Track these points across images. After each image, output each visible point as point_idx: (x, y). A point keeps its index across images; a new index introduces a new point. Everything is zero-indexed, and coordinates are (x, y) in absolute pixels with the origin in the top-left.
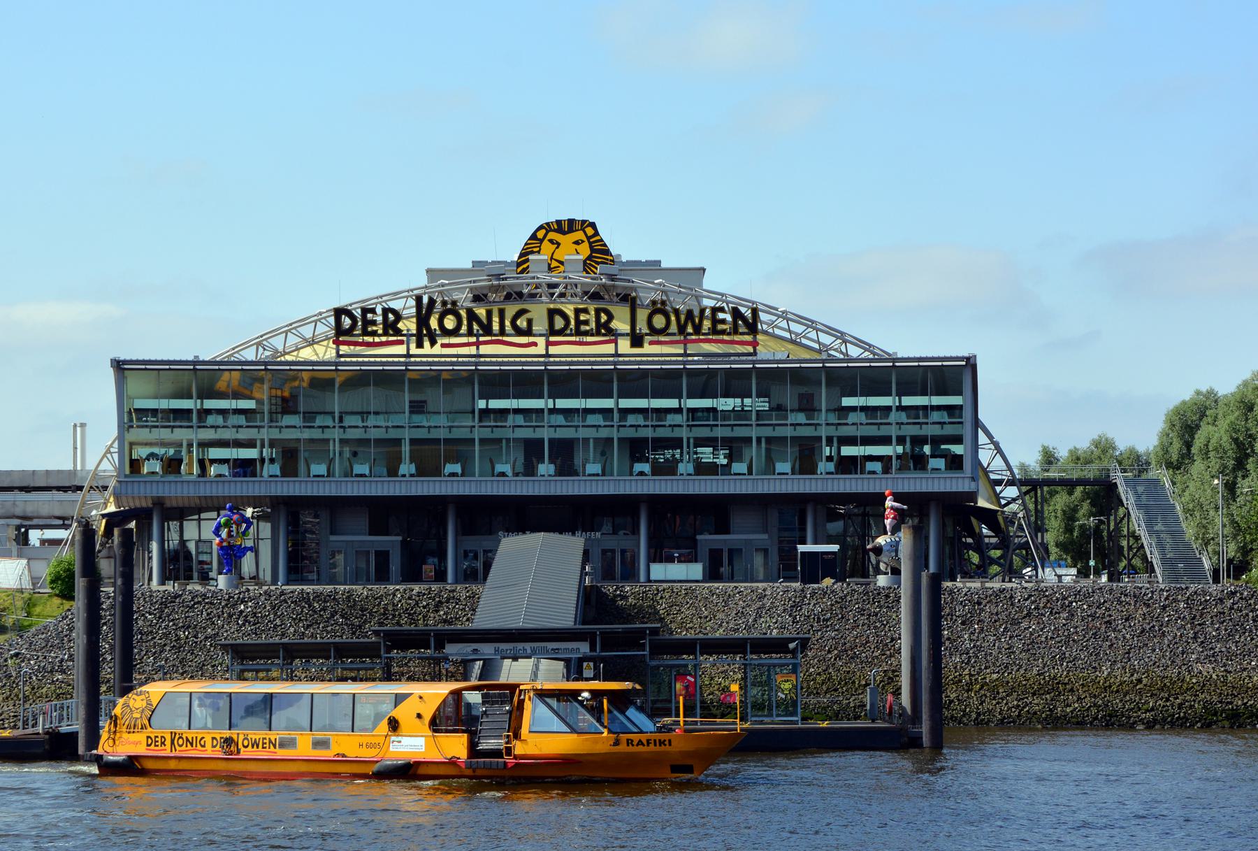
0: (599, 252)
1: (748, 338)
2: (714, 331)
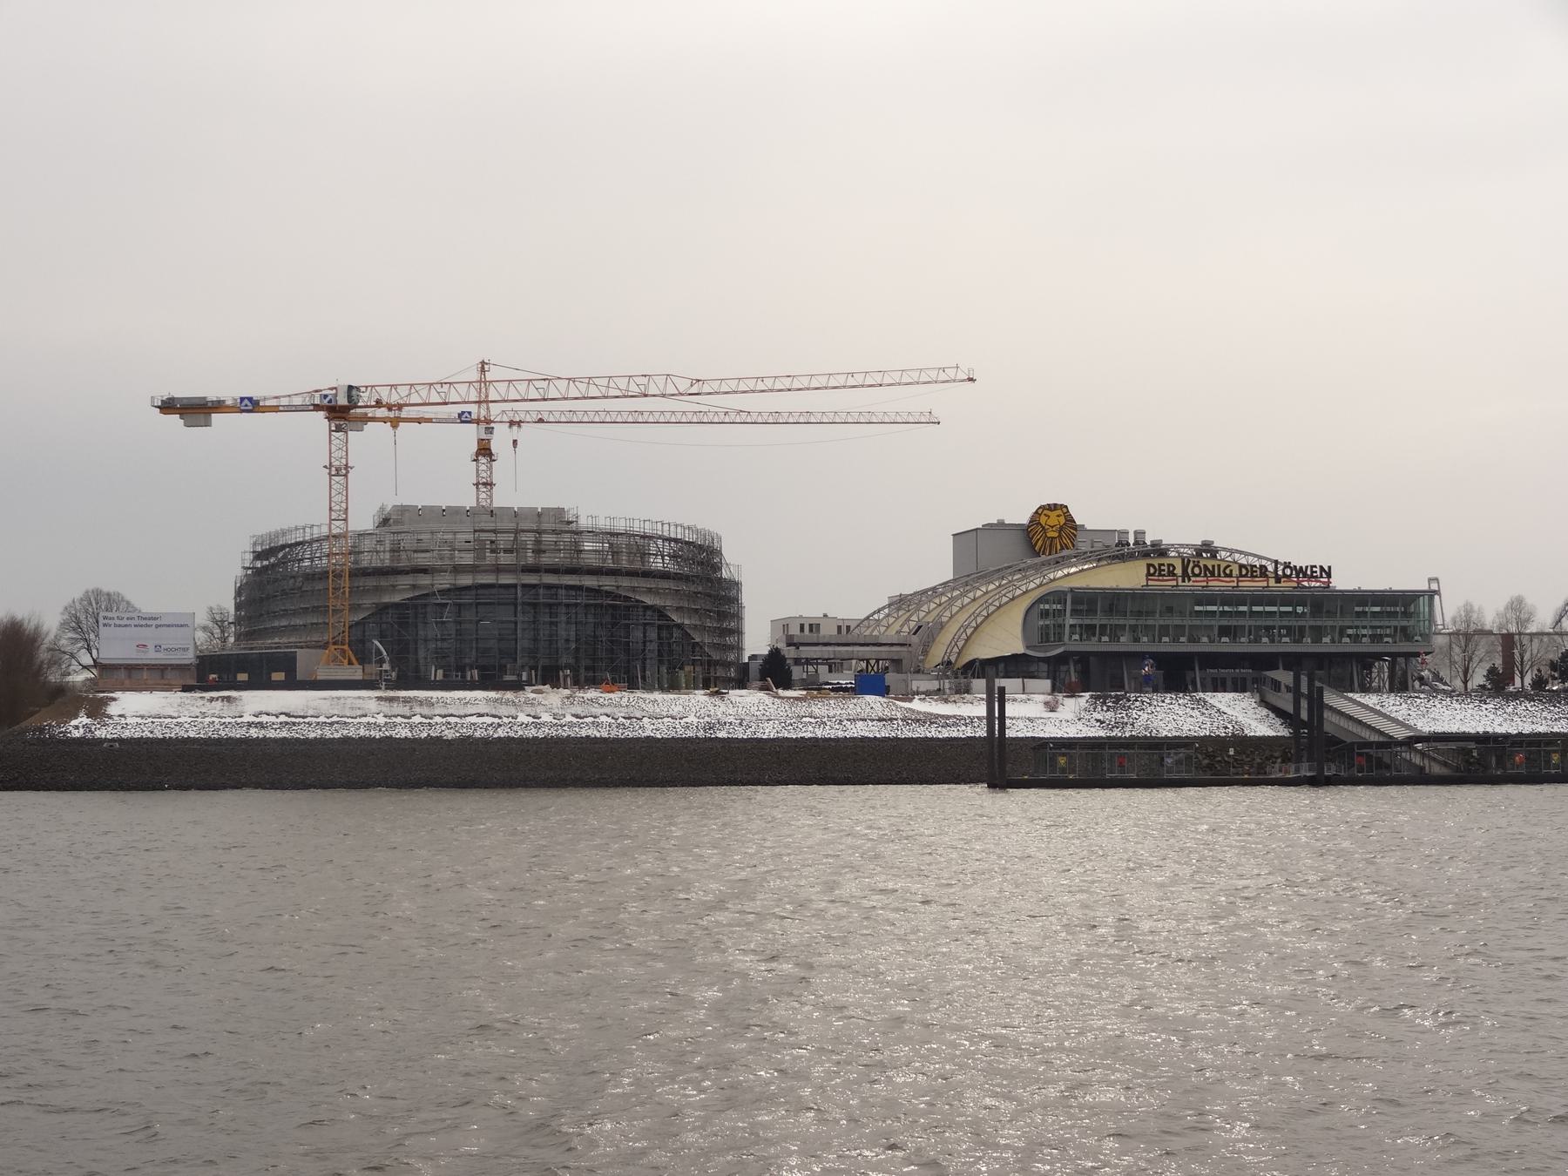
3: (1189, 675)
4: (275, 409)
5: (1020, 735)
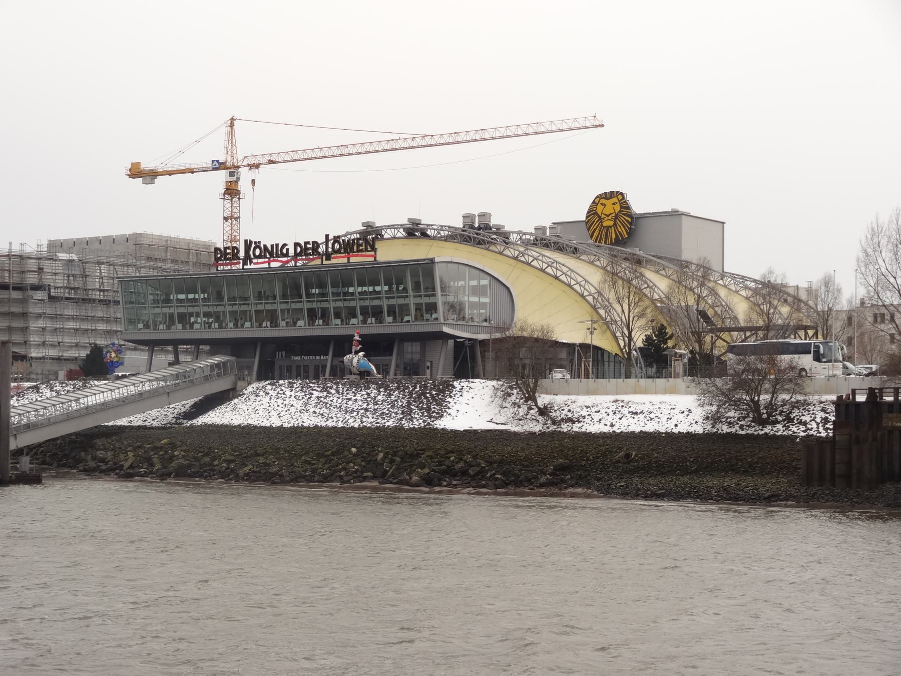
0: (625, 206)
1: (373, 253)
2: (358, 251)
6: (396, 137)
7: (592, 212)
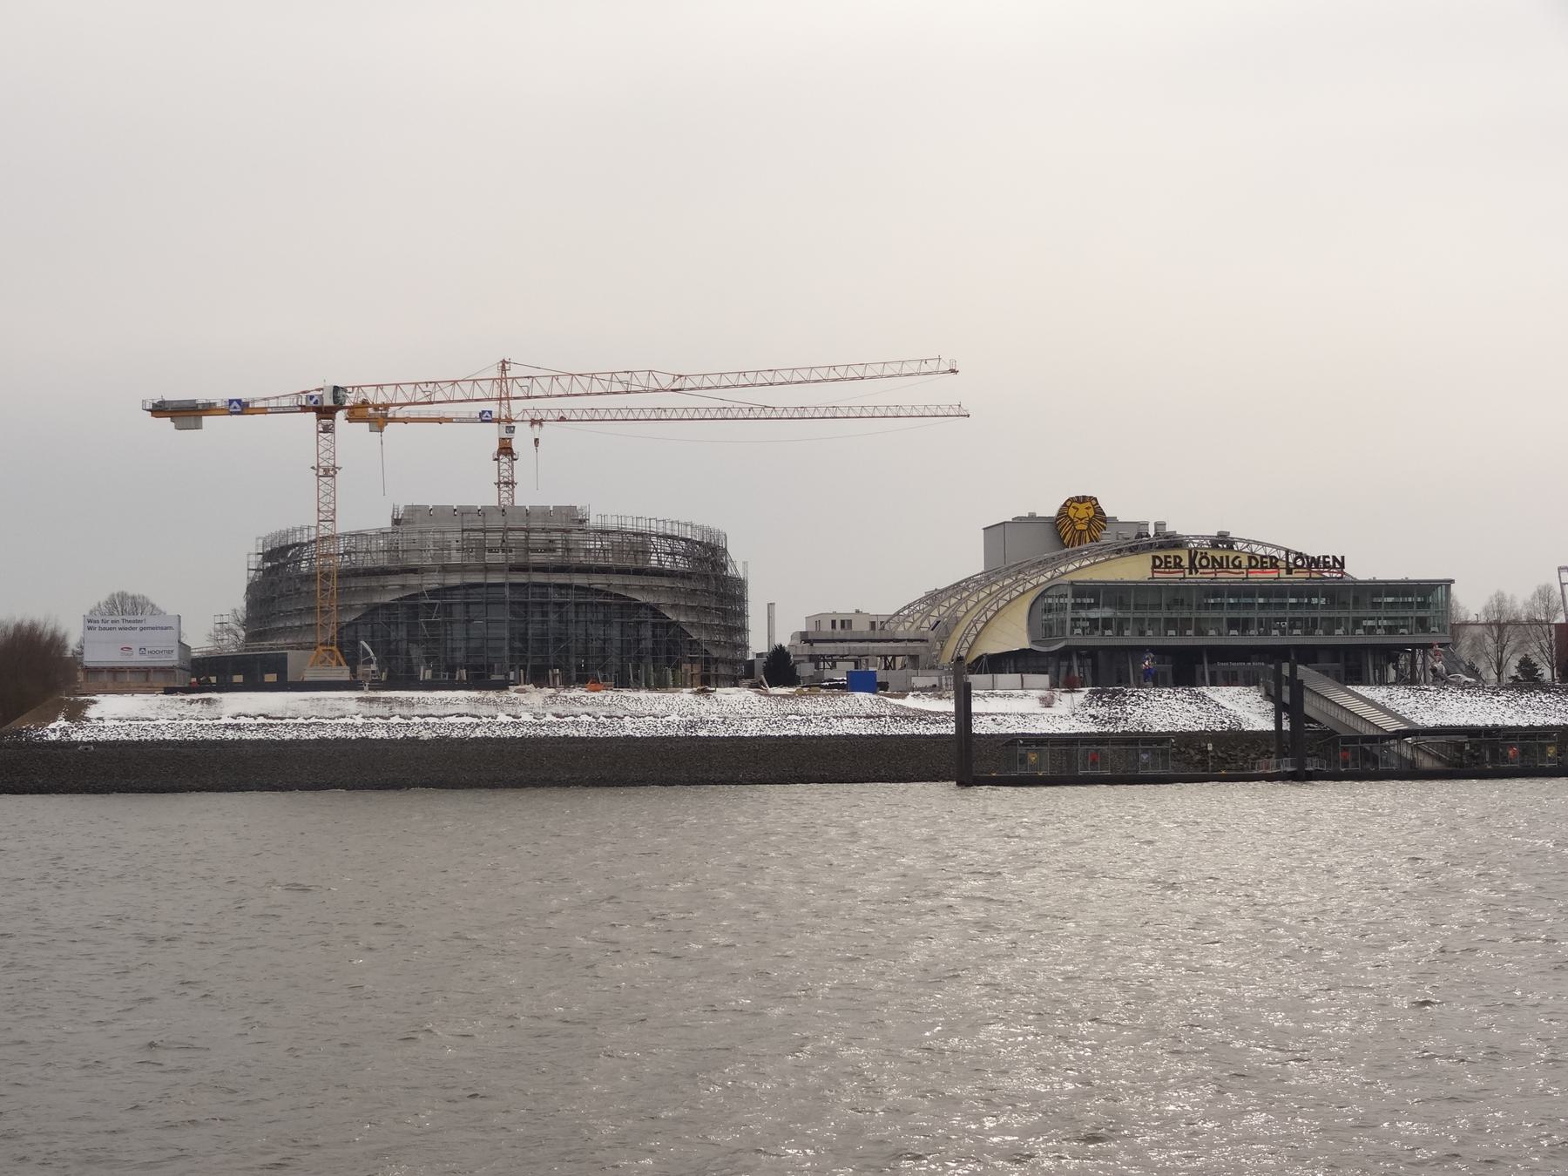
0: (1099, 512)
3: (1198, 668)
4: (264, 411)
5: (1011, 731)
6: (729, 405)
7: (1063, 512)
